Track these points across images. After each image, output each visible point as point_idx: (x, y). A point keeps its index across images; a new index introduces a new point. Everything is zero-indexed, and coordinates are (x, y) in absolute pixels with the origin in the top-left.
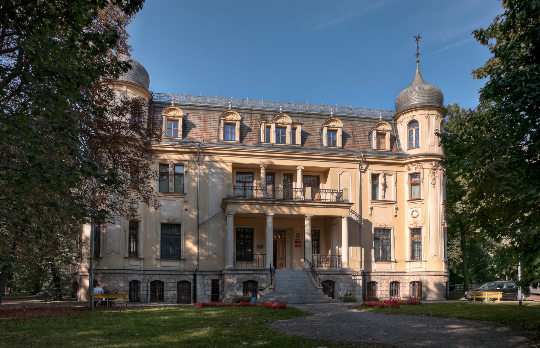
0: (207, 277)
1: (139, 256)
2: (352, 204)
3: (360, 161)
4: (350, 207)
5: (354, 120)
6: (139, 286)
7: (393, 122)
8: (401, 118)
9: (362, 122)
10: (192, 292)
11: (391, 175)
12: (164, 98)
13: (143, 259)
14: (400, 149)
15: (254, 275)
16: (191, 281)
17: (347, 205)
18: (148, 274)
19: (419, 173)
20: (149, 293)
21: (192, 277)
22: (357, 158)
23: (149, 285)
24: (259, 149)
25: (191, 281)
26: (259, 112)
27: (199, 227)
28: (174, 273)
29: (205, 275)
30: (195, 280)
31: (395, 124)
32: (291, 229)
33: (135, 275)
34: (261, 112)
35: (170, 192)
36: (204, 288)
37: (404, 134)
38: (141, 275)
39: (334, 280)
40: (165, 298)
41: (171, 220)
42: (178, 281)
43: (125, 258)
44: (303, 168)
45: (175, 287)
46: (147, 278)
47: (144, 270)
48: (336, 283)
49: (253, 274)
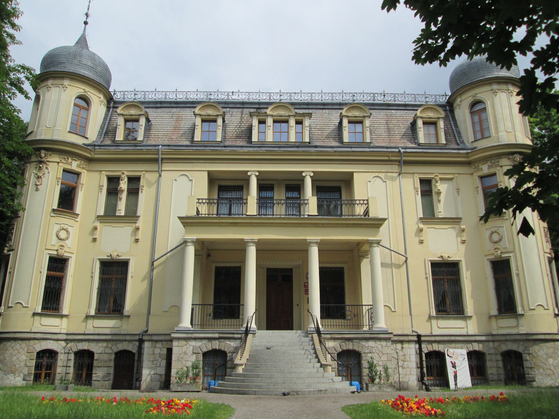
0: (159, 345)
1: (60, 311)
3: (399, 161)
4: (381, 225)
6: (56, 360)
7: (448, 108)
8: (458, 100)
11: (451, 179)
12: (129, 97)
13: (66, 316)
14: (463, 142)
17: (378, 223)
19: (494, 174)
20: (71, 370)
21: (137, 344)
22: (392, 156)
23: (72, 357)
24: (246, 150)
25: (135, 351)
29: (156, 341)
30: (140, 349)
31: (452, 111)
32: (299, 267)
33: (48, 341)
35: (117, 214)
36: (155, 362)
37: (465, 121)
38: (59, 342)
42: (116, 350)
43: (35, 314)
44: (312, 174)
45: (110, 360)
46: (69, 345)
47: (67, 334)
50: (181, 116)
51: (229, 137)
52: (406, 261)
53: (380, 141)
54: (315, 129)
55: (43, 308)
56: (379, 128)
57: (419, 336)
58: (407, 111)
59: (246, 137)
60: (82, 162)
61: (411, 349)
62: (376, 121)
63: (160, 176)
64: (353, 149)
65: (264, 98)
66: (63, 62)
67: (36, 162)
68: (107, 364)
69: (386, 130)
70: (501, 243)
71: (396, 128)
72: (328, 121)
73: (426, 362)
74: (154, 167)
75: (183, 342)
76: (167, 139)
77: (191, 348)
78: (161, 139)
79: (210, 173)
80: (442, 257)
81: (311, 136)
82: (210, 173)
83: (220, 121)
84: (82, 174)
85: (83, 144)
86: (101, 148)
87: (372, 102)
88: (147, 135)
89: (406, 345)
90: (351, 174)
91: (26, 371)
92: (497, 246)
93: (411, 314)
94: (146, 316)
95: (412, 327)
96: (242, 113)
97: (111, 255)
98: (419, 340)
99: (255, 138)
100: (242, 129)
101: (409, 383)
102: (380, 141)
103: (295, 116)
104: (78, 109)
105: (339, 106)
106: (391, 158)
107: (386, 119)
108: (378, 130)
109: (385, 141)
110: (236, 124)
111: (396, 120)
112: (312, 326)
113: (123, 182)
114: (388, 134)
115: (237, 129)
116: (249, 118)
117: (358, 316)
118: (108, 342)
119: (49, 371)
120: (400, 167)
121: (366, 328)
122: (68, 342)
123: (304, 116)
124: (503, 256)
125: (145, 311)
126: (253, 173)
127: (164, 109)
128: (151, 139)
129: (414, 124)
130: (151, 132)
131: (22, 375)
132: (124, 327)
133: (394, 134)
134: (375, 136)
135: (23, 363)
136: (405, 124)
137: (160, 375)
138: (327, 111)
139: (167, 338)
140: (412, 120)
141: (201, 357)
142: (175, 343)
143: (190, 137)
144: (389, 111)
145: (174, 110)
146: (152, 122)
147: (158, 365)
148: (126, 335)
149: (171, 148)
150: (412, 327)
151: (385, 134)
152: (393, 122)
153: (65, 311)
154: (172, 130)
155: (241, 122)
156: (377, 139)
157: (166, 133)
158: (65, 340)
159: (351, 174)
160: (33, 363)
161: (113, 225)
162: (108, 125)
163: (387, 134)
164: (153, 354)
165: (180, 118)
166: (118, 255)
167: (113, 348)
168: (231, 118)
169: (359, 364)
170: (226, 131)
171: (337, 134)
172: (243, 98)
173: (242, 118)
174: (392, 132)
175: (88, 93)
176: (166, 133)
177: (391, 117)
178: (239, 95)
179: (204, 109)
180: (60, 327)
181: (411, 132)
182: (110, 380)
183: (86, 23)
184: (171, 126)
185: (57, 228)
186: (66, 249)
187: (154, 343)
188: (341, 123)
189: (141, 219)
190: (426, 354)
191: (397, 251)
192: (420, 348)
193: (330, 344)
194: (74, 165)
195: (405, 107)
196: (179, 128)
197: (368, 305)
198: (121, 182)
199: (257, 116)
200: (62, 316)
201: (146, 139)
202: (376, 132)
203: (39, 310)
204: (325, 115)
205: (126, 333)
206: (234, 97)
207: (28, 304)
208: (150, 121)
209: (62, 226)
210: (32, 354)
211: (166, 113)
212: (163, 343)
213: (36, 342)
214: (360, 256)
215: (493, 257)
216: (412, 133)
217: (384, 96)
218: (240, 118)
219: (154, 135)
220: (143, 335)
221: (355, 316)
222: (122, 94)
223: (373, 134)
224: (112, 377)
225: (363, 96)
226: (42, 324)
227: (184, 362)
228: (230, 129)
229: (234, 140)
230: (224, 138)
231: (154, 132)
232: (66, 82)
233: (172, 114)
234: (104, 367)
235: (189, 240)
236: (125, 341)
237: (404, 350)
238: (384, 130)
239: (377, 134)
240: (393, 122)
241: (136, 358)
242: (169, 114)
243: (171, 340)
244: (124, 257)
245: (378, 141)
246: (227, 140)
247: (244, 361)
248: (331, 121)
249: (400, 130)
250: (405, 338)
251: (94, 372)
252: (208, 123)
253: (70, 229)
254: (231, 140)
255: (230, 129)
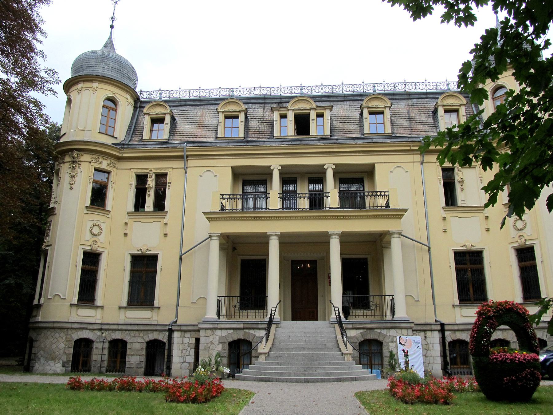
0: (188, 335)
2: (406, 210)
4: (403, 215)
5: (410, 99)
6: (92, 348)
9: (424, 100)
10: (166, 357)
12: (155, 96)
13: (102, 307)
15: (245, 330)
16: (165, 340)
17: (399, 214)
18: (106, 330)
20: (106, 358)
21: (167, 333)
22: (413, 146)
23: (106, 345)
24: (268, 144)
25: (165, 340)
26: (275, 101)
27: (181, 259)
28: (142, 327)
29: (185, 331)
30: (170, 338)
33: (84, 331)
34: (278, 101)
36: (184, 351)
38: (94, 331)
39: (381, 339)
40: (127, 366)
41: (144, 251)
42: (147, 339)
44: (334, 167)
45: (142, 349)
46: (104, 335)
47: (101, 324)
48: (384, 344)
49: (244, 328)
50: (205, 113)
51: (252, 133)
52: (429, 250)
53: (402, 131)
54: (336, 122)
55: (79, 300)
56: (400, 118)
57: (442, 325)
58: (428, 100)
59: (269, 132)
60: (112, 161)
61: (435, 338)
62: (397, 111)
63: (186, 172)
64: (374, 140)
65: (285, 93)
66: (92, 65)
67: (69, 162)
68: (140, 353)
69: (408, 120)
70: (525, 230)
71: (418, 117)
72: (349, 113)
73: (449, 350)
74: (180, 164)
75: (209, 332)
76: (192, 137)
77: (217, 337)
78: (186, 137)
79: (234, 169)
80: (465, 245)
81: (332, 129)
82: (234, 169)
83: (242, 116)
84: (112, 172)
85: (113, 144)
86: (129, 147)
87: (392, 91)
88: (173, 133)
89: (429, 334)
90: (373, 166)
91: (64, 358)
92: (520, 233)
93: (434, 303)
94: (175, 307)
95: (436, 316)
96: (264, 108)
97: (141, 249)
98: (442, 328)
99: (277, 133)
100: (264, 124)
101: (433, 371)
102: (402, 131)
103: (315, 109)
104: (107, 110)
105: (359, 97)
106: (413, 148)
107: (407, 109)
108: (399, 120)
109: (407, 131)
110: (258, 120)
111: (417, 109)
112: (333, 316)
113: (151, 179)
114: (410, 124)
115: (259, 124)
116: (270, 113)
117: (381, 305)
118: (140, 332)
119: (84, 359)
120: (422, 156)
121: (389, 318)
122: (103, 331)
123: (325, 109)
124: (527, 243)
125: (175, 303)
126: (276, 167)
127: (188, 107)
128: (177, 137)
129: (435, 112)
130: (177, 130)
131: (61, 362)
132: (155, 318)
133: (416, 124)
134: (397, 127)
135: (62, 351)
136: (426, 113)
137: (190, 363)
138: (348, 103)
139: (196, 328)
140: (434, 108)
141: (226, 346)
142: (202, 333)
143: (214, 134)
144: (410, 100)
145: (198, 108)
146: (177, 120)
147: (187, 354)
148: (156, 325)
149: (196, 145)
150: (436, 316)
151: (406, 124)
152: (414, 111)
153: (99, 302)
154: (196, 128)
155: (263, 117)
156: (399, 129)
157: (191, 130)
158: (101, 330)
159: (373, 166)
160: (71, 351)
161: (142, 220)
162: (135, 125)
163: (408, 124)
164: (182, 343)
165: (204, 115)
166: (147, 249)
167: (144, 338)
168: (253, 113)
169: (381, 353)
170: (249, 126)
171: (358, 126)
172: (265, 93)
173: (264, 113)
174: (413, 122)
175: (116, 95)
176: (191, 130)
177: (413, 107)
178: (260, 91)
179: (226, 106)
180: (95, 318)
181: (432, 121)
182: (142, 368)
183: (112, 27)
184: (196, 124)
185: (90, 224)
186: (99, 244)
187: (183, 333)
188: (361, 114)
189: (168, 215)
190: (450, 343)
191: (420, 241)
192: (443, 338)
193: (352, 333)
194: (105, 164)
195: (426, 95)
196: (204, 125)
197: (390, 296)
198: (149, 179)
199: (279, 111)
200: (98, 307)
201: (172, 137)
202: (397, 122)
203: (75, 301)
204: (346, 107)
205: (156, 324)
206: (256, 93)
207: (65, 296)
208: (176, 119)
209: (95, 222)
210: (70, 343)
211: (190, 111)
212: (192, 333)
213: (74, 331)
214: (383, 247)
215: (517, 244)
216: (434, 122)
217: (405, 85)
218: (262, 113)
219: (179, 133)
220: (172, 326)
221: (376, 306)
222: (148, 94)
223: (394, 124)
224: (143, 365)
225: (384, 86)
226: (79, 314)
227: (211, 351)
228: (253, 124)
229: (257, 135)
230: (247, 133)
231: (179, 130)
232: (95, 85)
233: (196, 111)
234: (137, 355)
235: (214, 235)
236: (156, 330)
237: (428, 339)
238: (406, 120)
239: (398, 124)
240: (414, 111)
241: (167, 347)
242: (193, 111)
243: (199, 331)
244: (153, 252)
245: (399, 131)
246: (250, 135)
247: (266, 350)
248: (352, 113)
249: (422, 119)
250: (428, 327)
251: (127, 360)
252: (231, 119)
253: (102, 225)
254: (253, 135)
255: (253, 124)
